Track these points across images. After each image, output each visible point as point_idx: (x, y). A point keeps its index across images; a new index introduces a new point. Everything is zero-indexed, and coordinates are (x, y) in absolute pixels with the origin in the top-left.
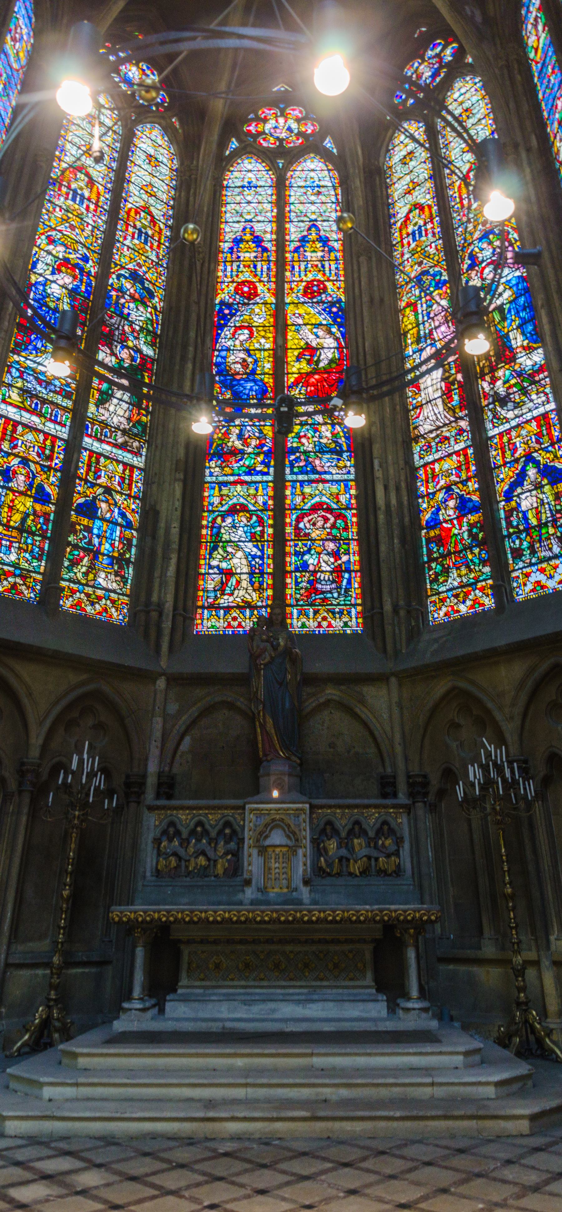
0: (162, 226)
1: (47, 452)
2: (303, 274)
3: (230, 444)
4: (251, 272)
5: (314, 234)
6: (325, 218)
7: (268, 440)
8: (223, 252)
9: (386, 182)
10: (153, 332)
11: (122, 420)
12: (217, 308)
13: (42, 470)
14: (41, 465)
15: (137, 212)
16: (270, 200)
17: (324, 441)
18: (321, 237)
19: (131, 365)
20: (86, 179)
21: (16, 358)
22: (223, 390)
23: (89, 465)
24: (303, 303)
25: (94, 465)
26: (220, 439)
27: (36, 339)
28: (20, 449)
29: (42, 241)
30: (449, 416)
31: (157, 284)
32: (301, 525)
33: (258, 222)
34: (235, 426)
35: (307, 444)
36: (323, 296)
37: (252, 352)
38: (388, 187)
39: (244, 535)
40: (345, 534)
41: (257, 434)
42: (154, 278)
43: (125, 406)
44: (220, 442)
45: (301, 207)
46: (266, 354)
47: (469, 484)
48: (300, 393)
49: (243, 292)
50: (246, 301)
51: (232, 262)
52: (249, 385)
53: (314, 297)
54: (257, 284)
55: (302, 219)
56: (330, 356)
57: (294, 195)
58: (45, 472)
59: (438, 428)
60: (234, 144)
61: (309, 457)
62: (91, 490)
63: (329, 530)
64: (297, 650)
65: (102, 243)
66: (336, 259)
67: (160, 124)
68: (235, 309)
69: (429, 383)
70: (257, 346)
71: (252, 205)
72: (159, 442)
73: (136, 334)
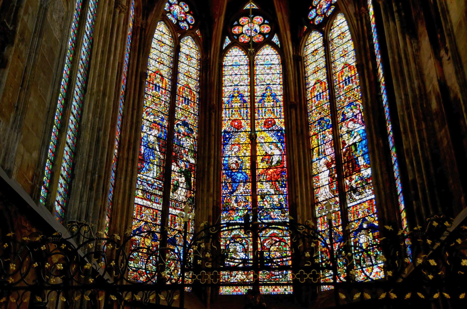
0: (195, 93)
1: (155, 217)
2: (263, 115)
3: (232, 205)
4: (239, 114)
5: (269, 92)
6: (274, 83)
7: (249, 203)
8: (224, 103)
9: (304, 64)
10: (194, 151)
11: (184, 198)
12: (223, 134)
13: (153, 226)
14: (153, 224)
15: (183, 89)
16: (246, 73)
17: (275, 203)
18: (272, 93)
19: (185, 169)
20: (160, 77)
22: (228, 177)
23: (171, 221)
24: (264, 131)
25: (173, 220)
26: (226, 202)
29: (144, 115)
30: (331, 195)
31: (195, 125)
32: (265, 244)
33: (241, 85)
34: (234, 196)
35: (267, 205)
36: (274, 127)
37: (240, 158)
39: (239, 249)
40: (285, 248)
41: (244, 200)
42: (193, 122)
43: (184, 190)
44: (227, 204)
45: (262, 76)
46: (247, 158)
47: (339, 228)
48: (264, 179)
49: (235, 125)
50: (236, 130)
51: (229, 109)
52: (239, 175)
53: (270, 127)
54: (242, 121)
55: (263, 83)
56: (277, 159)
57: (258, 69)
58: (155, 227)
59: (326, 200)
60: (228, 41)
62: (173, 232)
63: (277, 247)
64: (264, 304)
65: (169, 109)
66: (280, 106)
67: (191, 36)
68: (231, 135)
69: (323, 177)
70: (243, 154)
71: (237, 76)
72: (200, 207)
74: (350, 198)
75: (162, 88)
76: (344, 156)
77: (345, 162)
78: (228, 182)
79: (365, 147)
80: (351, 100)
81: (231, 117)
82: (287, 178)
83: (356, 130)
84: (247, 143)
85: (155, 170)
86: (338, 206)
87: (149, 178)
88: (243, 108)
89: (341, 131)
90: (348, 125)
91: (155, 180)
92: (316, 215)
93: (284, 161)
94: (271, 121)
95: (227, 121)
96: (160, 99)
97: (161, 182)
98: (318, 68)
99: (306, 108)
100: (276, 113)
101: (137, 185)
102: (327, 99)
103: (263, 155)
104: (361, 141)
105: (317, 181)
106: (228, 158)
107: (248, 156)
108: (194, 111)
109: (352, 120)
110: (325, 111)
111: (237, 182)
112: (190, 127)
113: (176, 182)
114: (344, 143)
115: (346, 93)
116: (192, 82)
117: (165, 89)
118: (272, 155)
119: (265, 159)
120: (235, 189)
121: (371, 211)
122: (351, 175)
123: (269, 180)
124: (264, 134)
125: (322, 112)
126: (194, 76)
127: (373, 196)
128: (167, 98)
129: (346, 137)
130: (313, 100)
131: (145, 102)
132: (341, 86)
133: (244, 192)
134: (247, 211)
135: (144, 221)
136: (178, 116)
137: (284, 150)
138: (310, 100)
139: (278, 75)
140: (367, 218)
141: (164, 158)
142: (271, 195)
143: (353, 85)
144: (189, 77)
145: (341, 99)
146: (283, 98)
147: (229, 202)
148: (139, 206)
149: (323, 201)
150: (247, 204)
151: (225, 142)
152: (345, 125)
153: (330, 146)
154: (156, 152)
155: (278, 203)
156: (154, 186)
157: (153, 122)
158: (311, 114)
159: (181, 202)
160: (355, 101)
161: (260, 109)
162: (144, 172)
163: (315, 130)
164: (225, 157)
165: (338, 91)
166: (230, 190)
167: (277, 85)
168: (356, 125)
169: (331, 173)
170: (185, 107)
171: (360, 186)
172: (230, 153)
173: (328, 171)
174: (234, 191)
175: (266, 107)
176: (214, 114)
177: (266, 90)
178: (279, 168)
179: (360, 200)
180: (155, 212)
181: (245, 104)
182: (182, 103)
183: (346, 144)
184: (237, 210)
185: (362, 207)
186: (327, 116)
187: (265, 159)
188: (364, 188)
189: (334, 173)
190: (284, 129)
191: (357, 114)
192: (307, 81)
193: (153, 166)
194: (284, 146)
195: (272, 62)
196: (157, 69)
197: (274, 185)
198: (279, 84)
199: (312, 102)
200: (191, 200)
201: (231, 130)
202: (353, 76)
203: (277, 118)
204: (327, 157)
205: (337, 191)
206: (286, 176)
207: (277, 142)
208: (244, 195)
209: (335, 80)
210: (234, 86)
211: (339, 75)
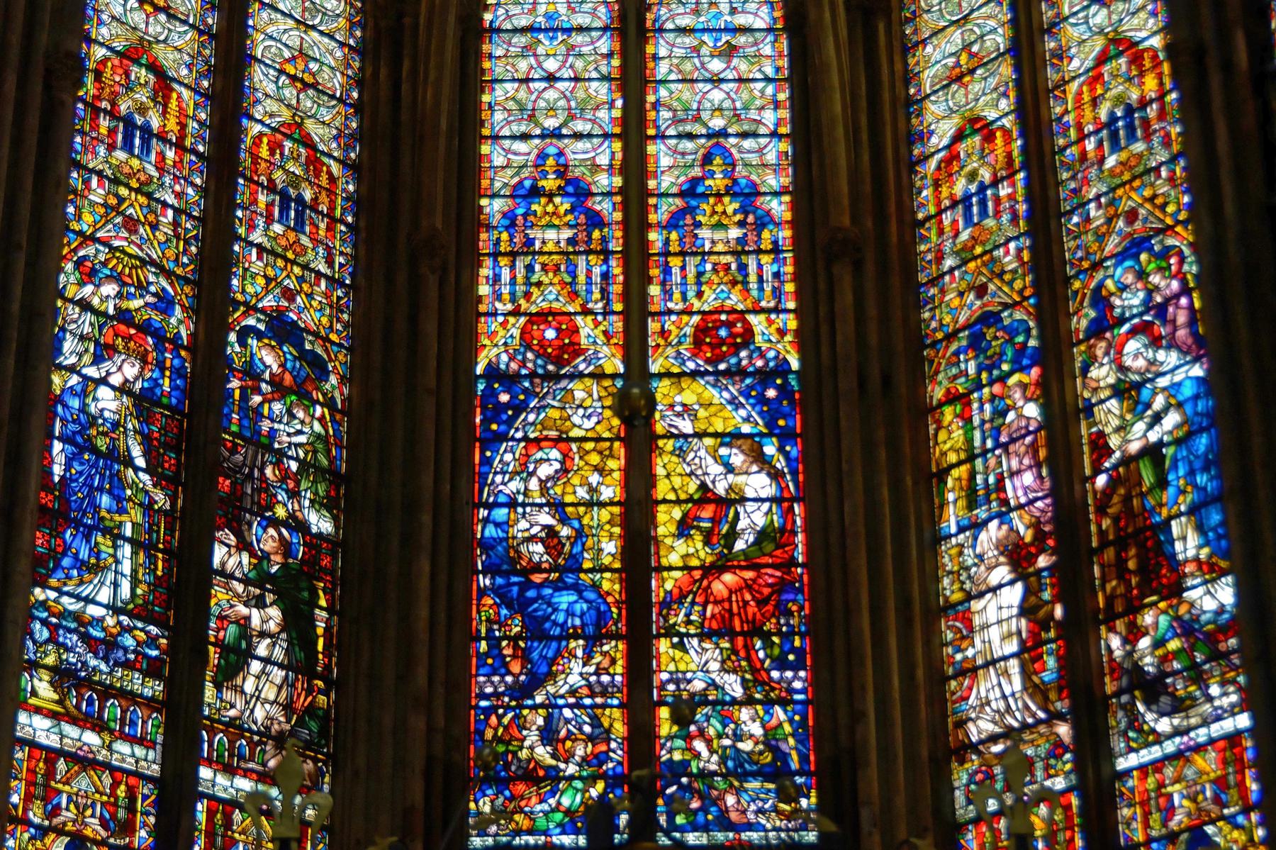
0: (336, 169)
1: (121, 814)
3: (524, 754)
4: (563, 284)
6: (746, 127)
7: (613, 745)
8: (489, 227)
11: (275, 711)
12: (481, 386)
16: (604, 70)
17: (746, 746)
18: (735, 181)
19: (284, 566)
22: (504, 612)
24: (694, 374)
28: (68, 815)
30: (1033, 707)
31: (333, 337)
33: (578, 136)
34: (534, 707)
35: (705, 753)
36: (743, 354)
37: (570, 510)
38: (908, 48)
41: (587, 729)
42: (325, 320)
43: (278, 674)
46: (605, 514)
50: (551, 367)
52: (565, 599)
53: (721, 358)
54: (579, 320)
55: (688, 128)
56: (760, 520)
59: (1009, 733)
61: (711, 787)
66: (776, 250)
68: (525, 391)
70: (582, 493)
71: (559, 85)
73: (291, 485)
74: (1130, 726)
75: (162, 137)
76: (1101, 511)
77: (1104, 544)
78: (505, 637)
79: (1206, 469)
80: (1138, 225)
81: (522, 302)
82: (809, 620)
83: (1163, 382)
84: (606, 435)
85: (126, 567)
86: (1068, 767)
87: (94, 611)
88: (588, 252)
89: (1084, 386)
90: (1120, 353)
91: (125, 620)
92: (954, 810)
93: (795, 534)
94: (729, 325)
95: (500, 319)
96: (149, 196)
97: (154, 630)
98: (972, 55)
99: (909, 263)
100: (753, 286)
101: (30, 644)
102: (1014, 219)
103: (686, 501)
104: (1190, 435)
105: (963, 638)
106: (505, 511)
107: (612, 503)
108: (330, 262)
109: (1142, 329)
110: (1007, 277)
111: (553, 638)
112: (308, 347)
113: (232, 629)
114: (1100, 446)
115: (1113, 190)
116: (323, 111)
117: (180, 146)
118: (734, 502)
119: (699, 519)
120: (544, 669)
121: (1234, 793)
122: (1135, 608)
123: (715, 625)
124: (689, 394)
125: (991, 287)
126: (335, 82)
127: (1243, 721)
128: (190, 191)
129: (1110, 412)
130: (947, 219)
131: (71, 210)
132: (1091, 155)
133: (589, 686)
134: (600, 786)
135: (67, 834)
136: (250, 289)
137: (794, 473)
138: (928, 218)
139: (770, 90)
140: (1210, 829)
141: (173, 504)
142: (724, 706)
143: (1150, 149)
144: (306, 86)
145: (1088, 220)
146: (794, 206)
147: (512, 738)
148: (37, 753)
149: (994, 739)
150: (603, 748)
151: (494, 427)
152: (1107, 353)
153: (1026, 461)
154: (130, 472)
155: (761, 747)
156: (120, 653)
157: (112, 318)
158: (933, 291)
159: (259, 733)
160: (1158, 232)
161: (675, 262)
162: (69, 577)
163: (955, 377)
164: (490, 507)
165: (1073, 178)
166: (516, 676)
167: (763, 141)
168: (1161, 355)
169: (1033, 599)
170: (284, 242)
171: (1176, 665)
172: (515, 485)
173: (1019, 586)
174: (536, 681)
175: (704, 253)
176: (433, 280)
177: (703, 165)
178: (767, 566)
179: (1177, 740)
180: (123, 787)
181: (596, 234)
182: (269, 220)
183: (1110, 452)
184: (553, 778)
185: (1189, 772)
186: (1015, 305)
187: (699, 519)
188: (1198, 676)
189: (1046, 595)
190: (795, 364)
191: (1167, 301)
192: (914, 121)
193: (115, 547)
194: (794, 453)
195: (740, 20)
196: (134, 37)
197: (742, 654)
198: (774, 134)
199: (941, 232)
200: (314, 726)
201: (523, 364)
202: (1152, 101)
203: (757, 311)
204: (1014, 515)
205: (1060, 690)
206: (801, 608)
207: (761, 435)
208: (587, 701)
209: (1060, 119)
210: (542, 137)
211: (1079, 93)
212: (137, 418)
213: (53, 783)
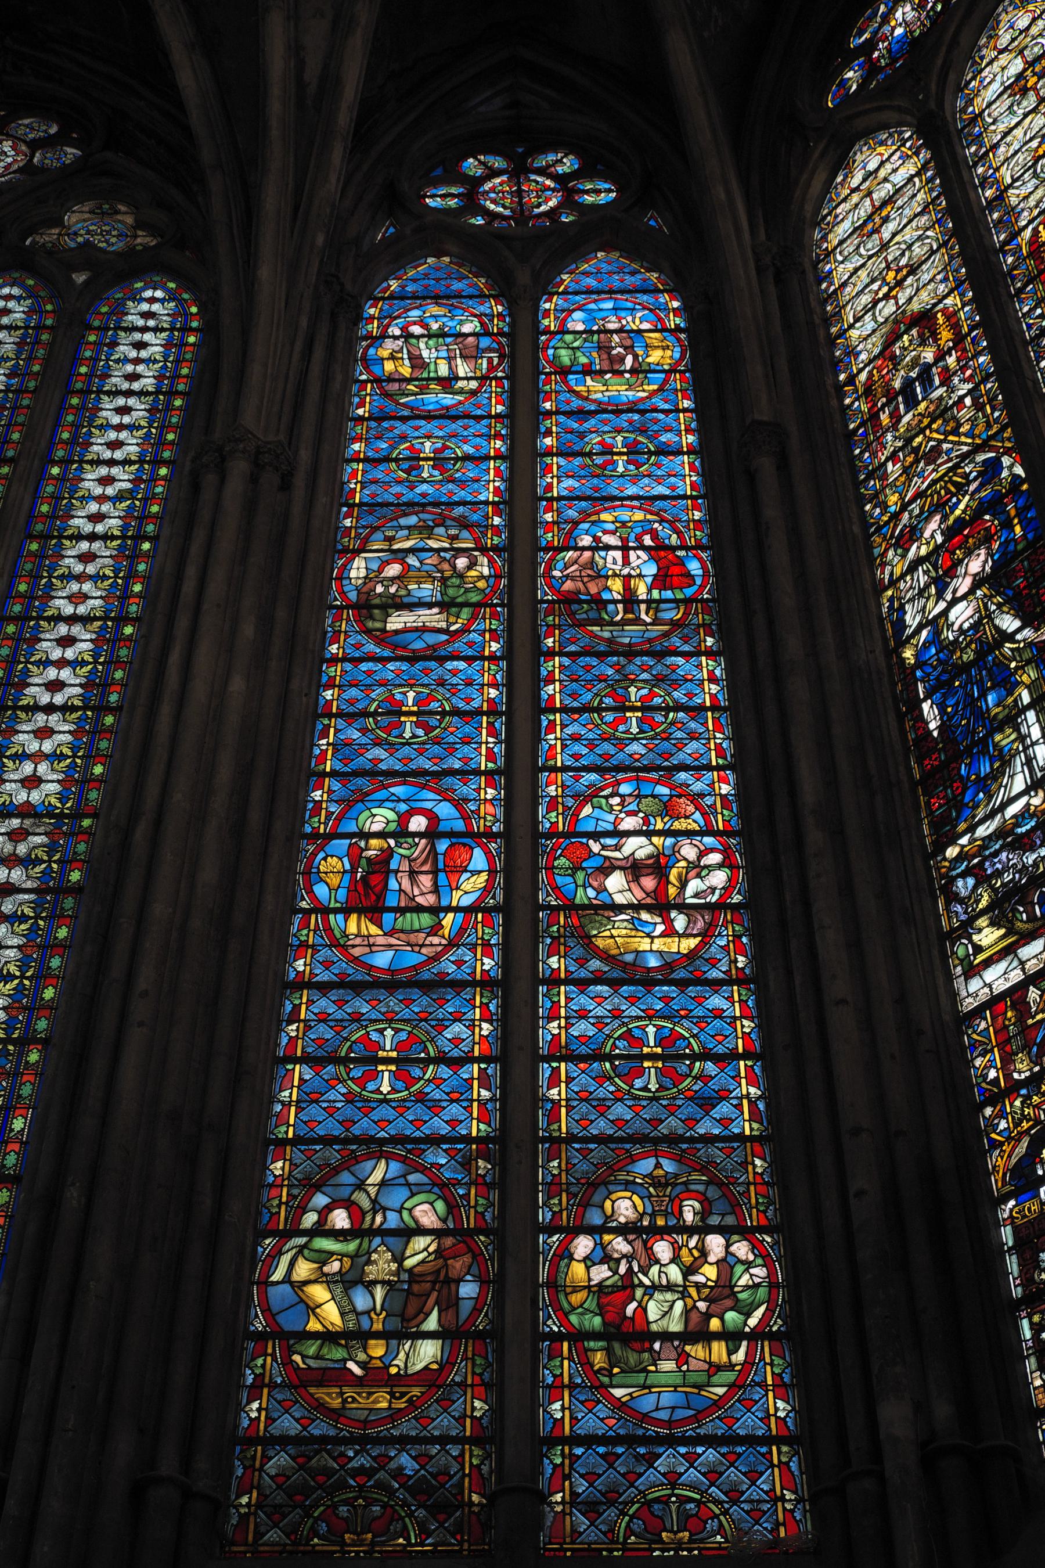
21: (952, 852)
27: (969, 766)
212: (999, 594)
213: (1030, 1022)
